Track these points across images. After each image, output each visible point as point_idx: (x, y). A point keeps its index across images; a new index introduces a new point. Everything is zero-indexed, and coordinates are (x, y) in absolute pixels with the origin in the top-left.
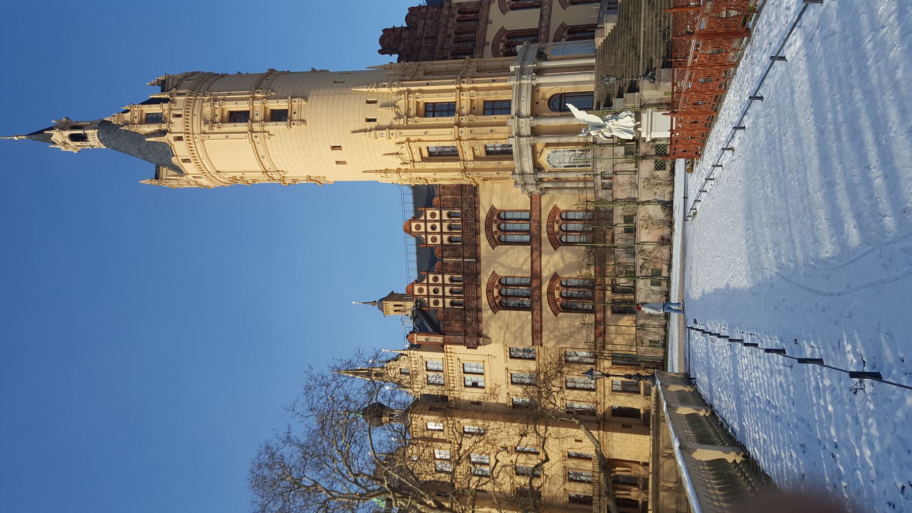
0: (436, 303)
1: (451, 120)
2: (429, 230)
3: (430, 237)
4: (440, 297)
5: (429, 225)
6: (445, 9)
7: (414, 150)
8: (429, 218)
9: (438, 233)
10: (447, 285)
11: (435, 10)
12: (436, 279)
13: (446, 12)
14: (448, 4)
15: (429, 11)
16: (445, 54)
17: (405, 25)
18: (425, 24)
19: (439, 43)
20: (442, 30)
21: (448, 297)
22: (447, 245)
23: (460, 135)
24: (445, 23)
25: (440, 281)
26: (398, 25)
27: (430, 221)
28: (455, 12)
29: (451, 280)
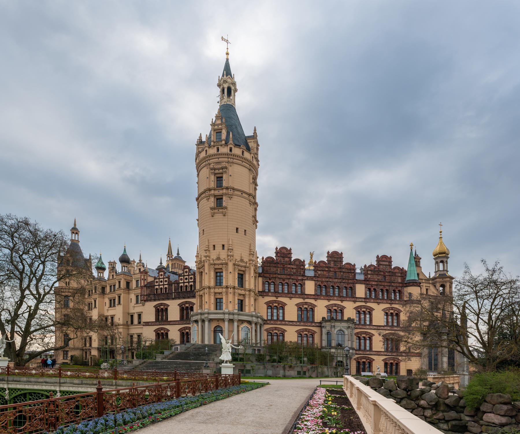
0: (157, 282)
1: (212, 284)
2: (185, 277)
3: (182, 277)
4: (159, 284)
5: (187, 277)
6: (302, 277)
8: (190, 277)
9: (184, 281)
10: (164, 286)
11: (302, 273)
12: (166, 281)
13: (300, 278)
14: (304, 279)
16: (272, 279)
18: (293, 268)
19: (279, 276)
20: (289, 277)
21: (159, 287)
22: (179, 286)
25: (165, 283)
27: (189, 277)
28: (300, 282)
29: (166, 288)
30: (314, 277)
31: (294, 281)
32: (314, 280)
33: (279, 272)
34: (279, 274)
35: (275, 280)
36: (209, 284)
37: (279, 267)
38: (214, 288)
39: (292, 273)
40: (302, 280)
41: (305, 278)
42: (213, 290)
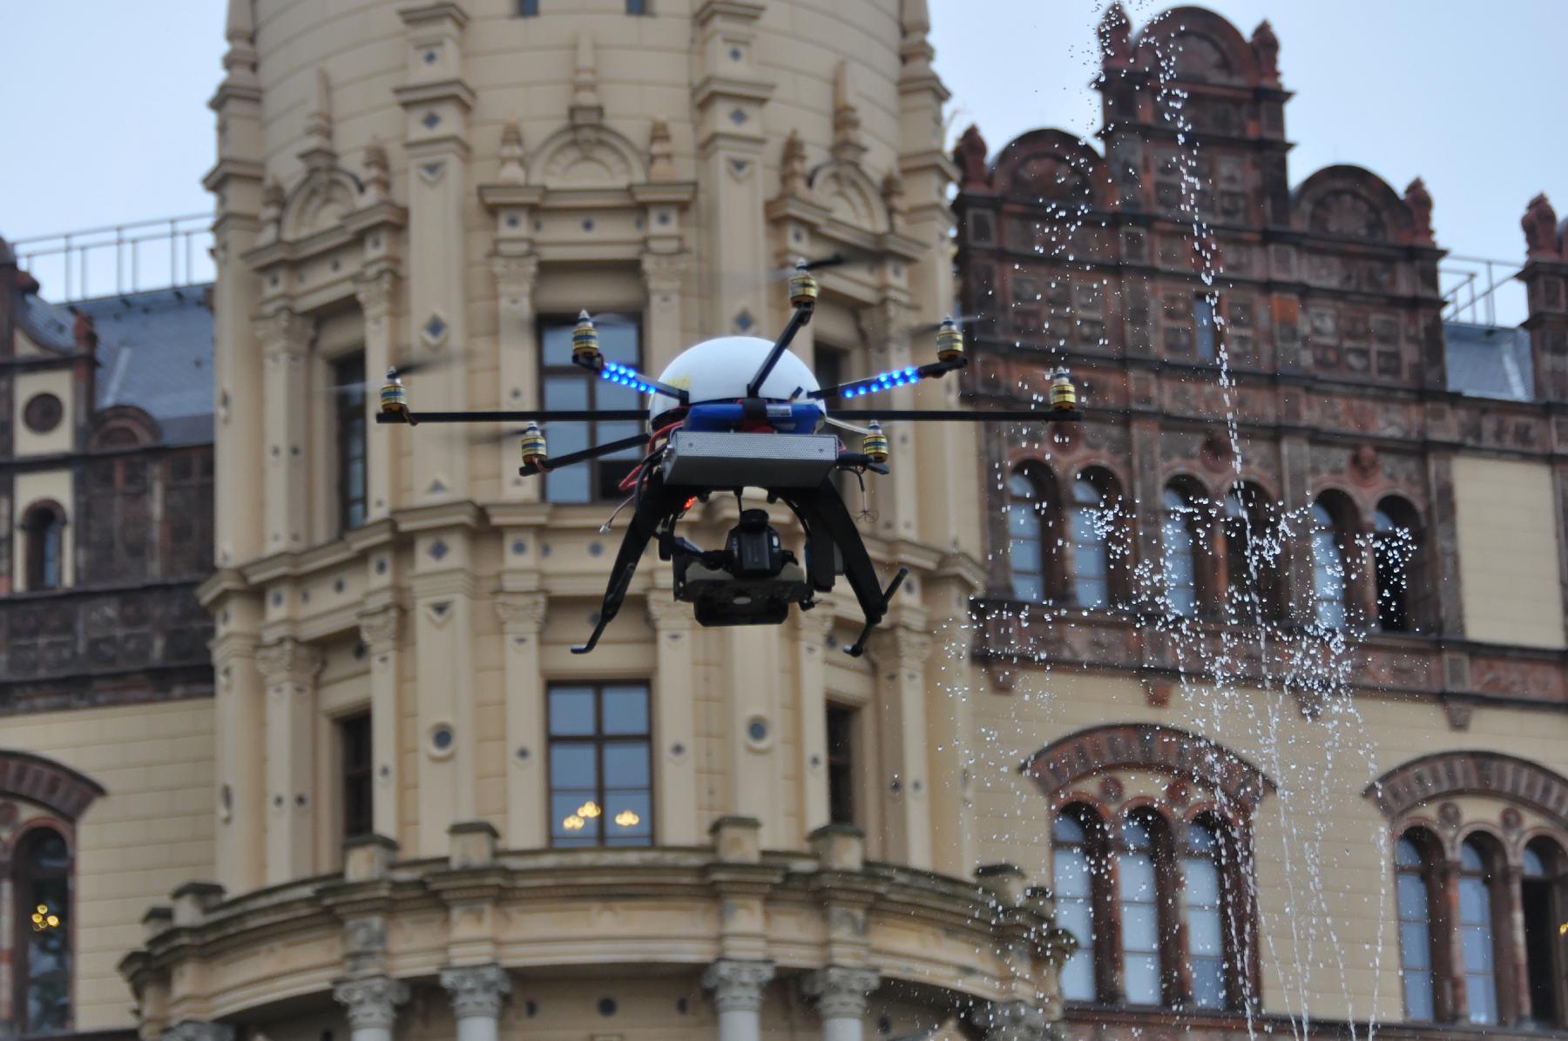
7: (350, 265)
11: (1409, 354)
13: (1390, 423)
15: (1402, 317)
17: (1298, 170)
18: (1305, 292)
19: (1165, 395)
23: (510, 540)
24: (1311, 414)
26: (1296, 121)
28: (1393, 477)
30: (1543, 409)
31: (1331, 471)
32: (1551, 459)
33: (1157, 347)
34: (1162, 369)
35: (1124, 446)
36: (474, 478)
37: (1152, 272)
38: (541, 530)
39: (1307, 358)
40: (1421, 449)
41: (1448, 428)
42: (529, 559)
